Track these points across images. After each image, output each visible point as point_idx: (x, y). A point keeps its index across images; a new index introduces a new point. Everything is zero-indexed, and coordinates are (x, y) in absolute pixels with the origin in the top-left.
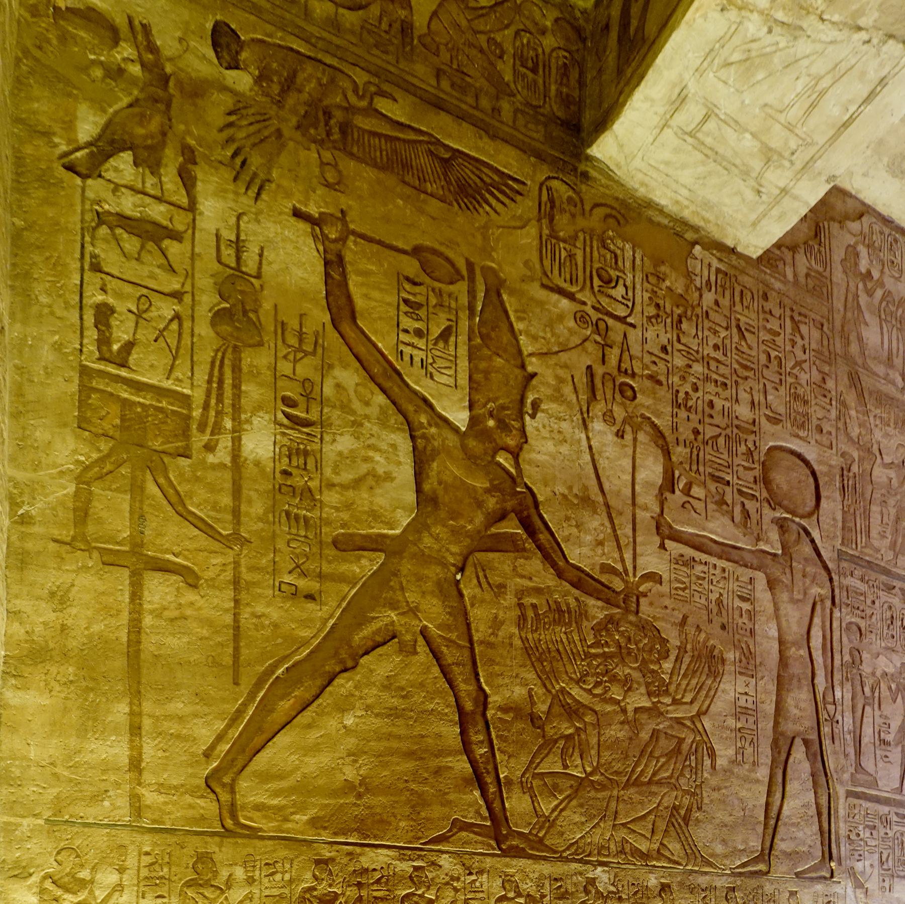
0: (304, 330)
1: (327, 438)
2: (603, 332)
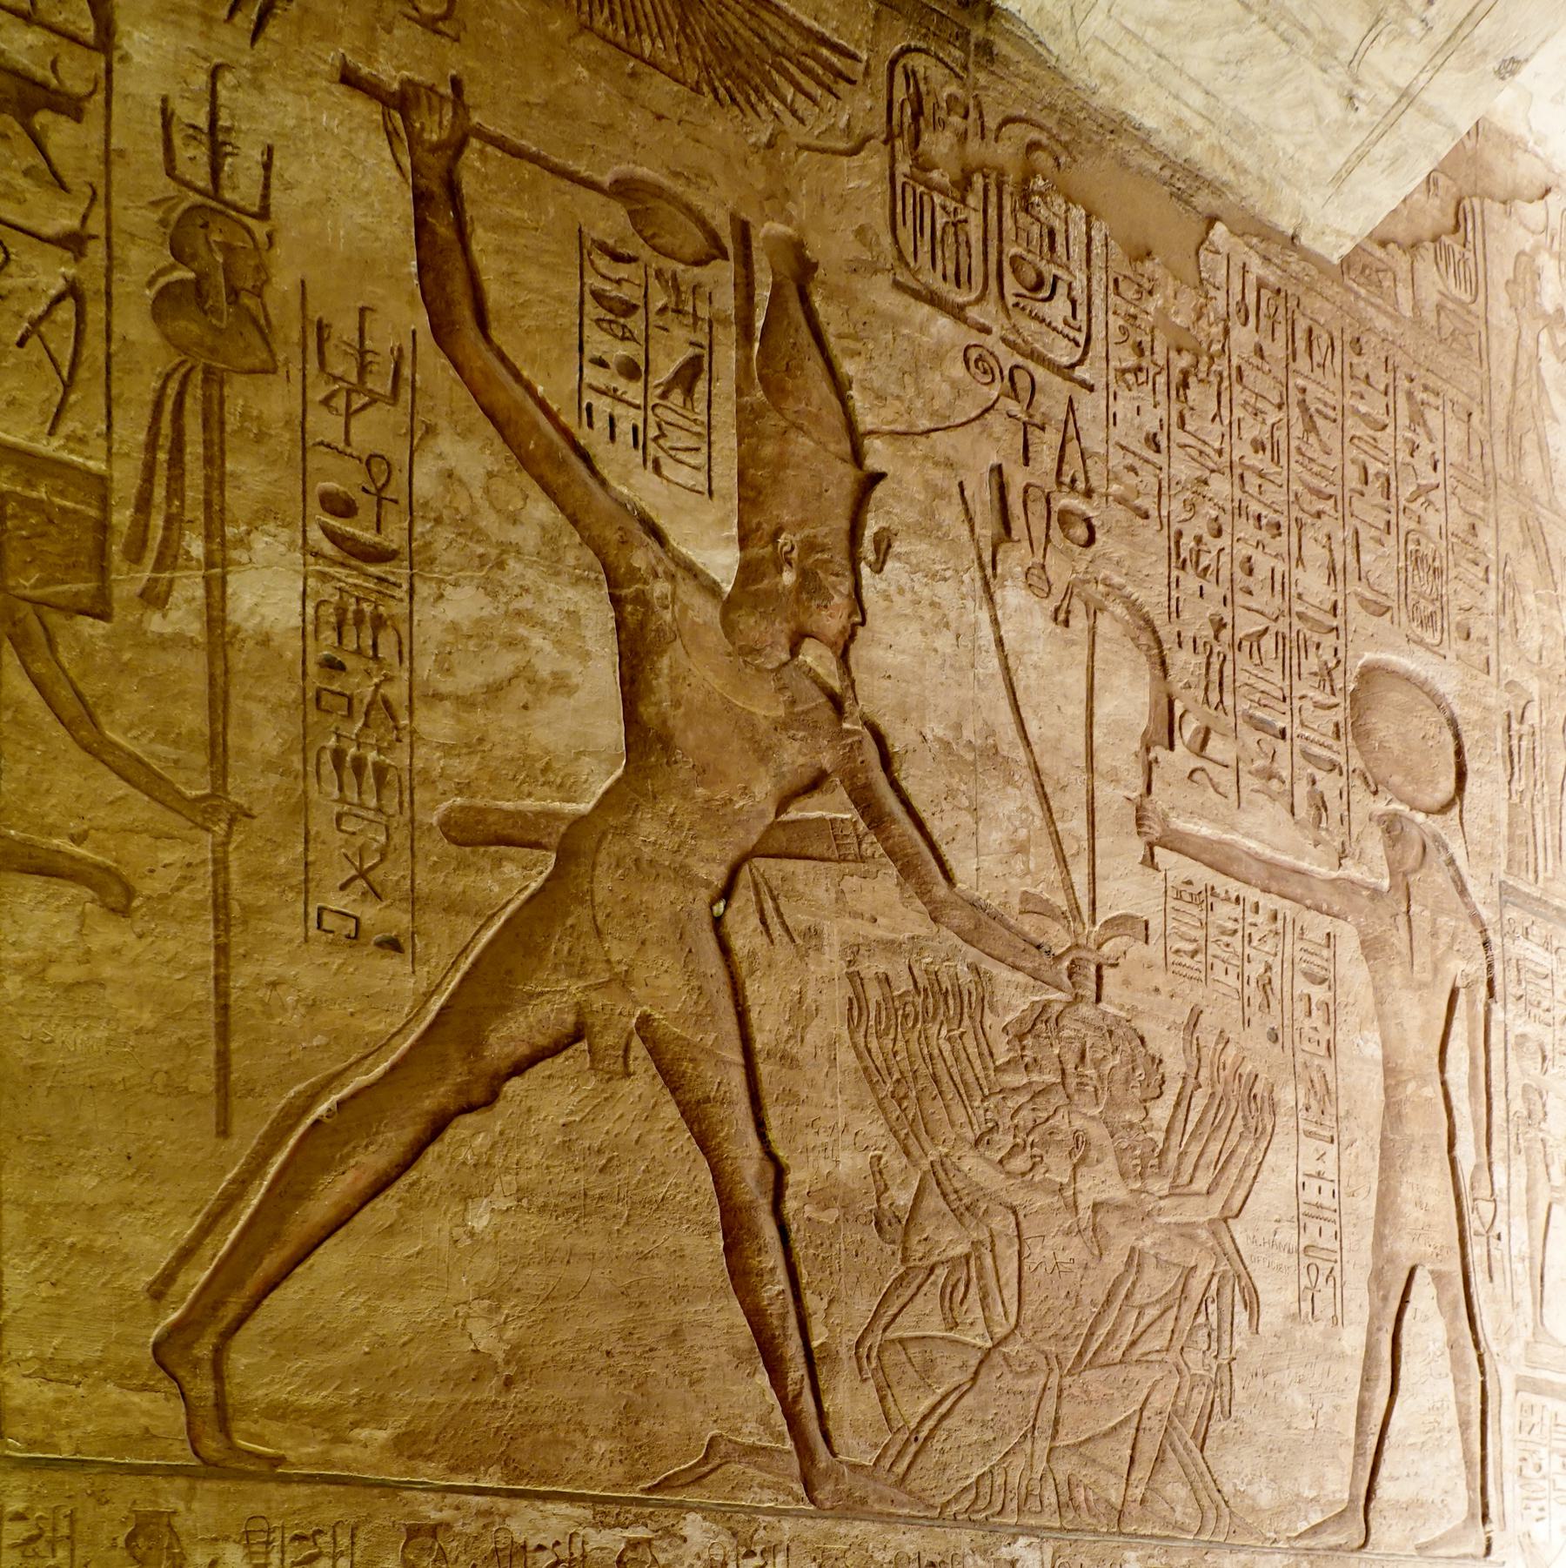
0: (368, 344)
1: (423, 590)
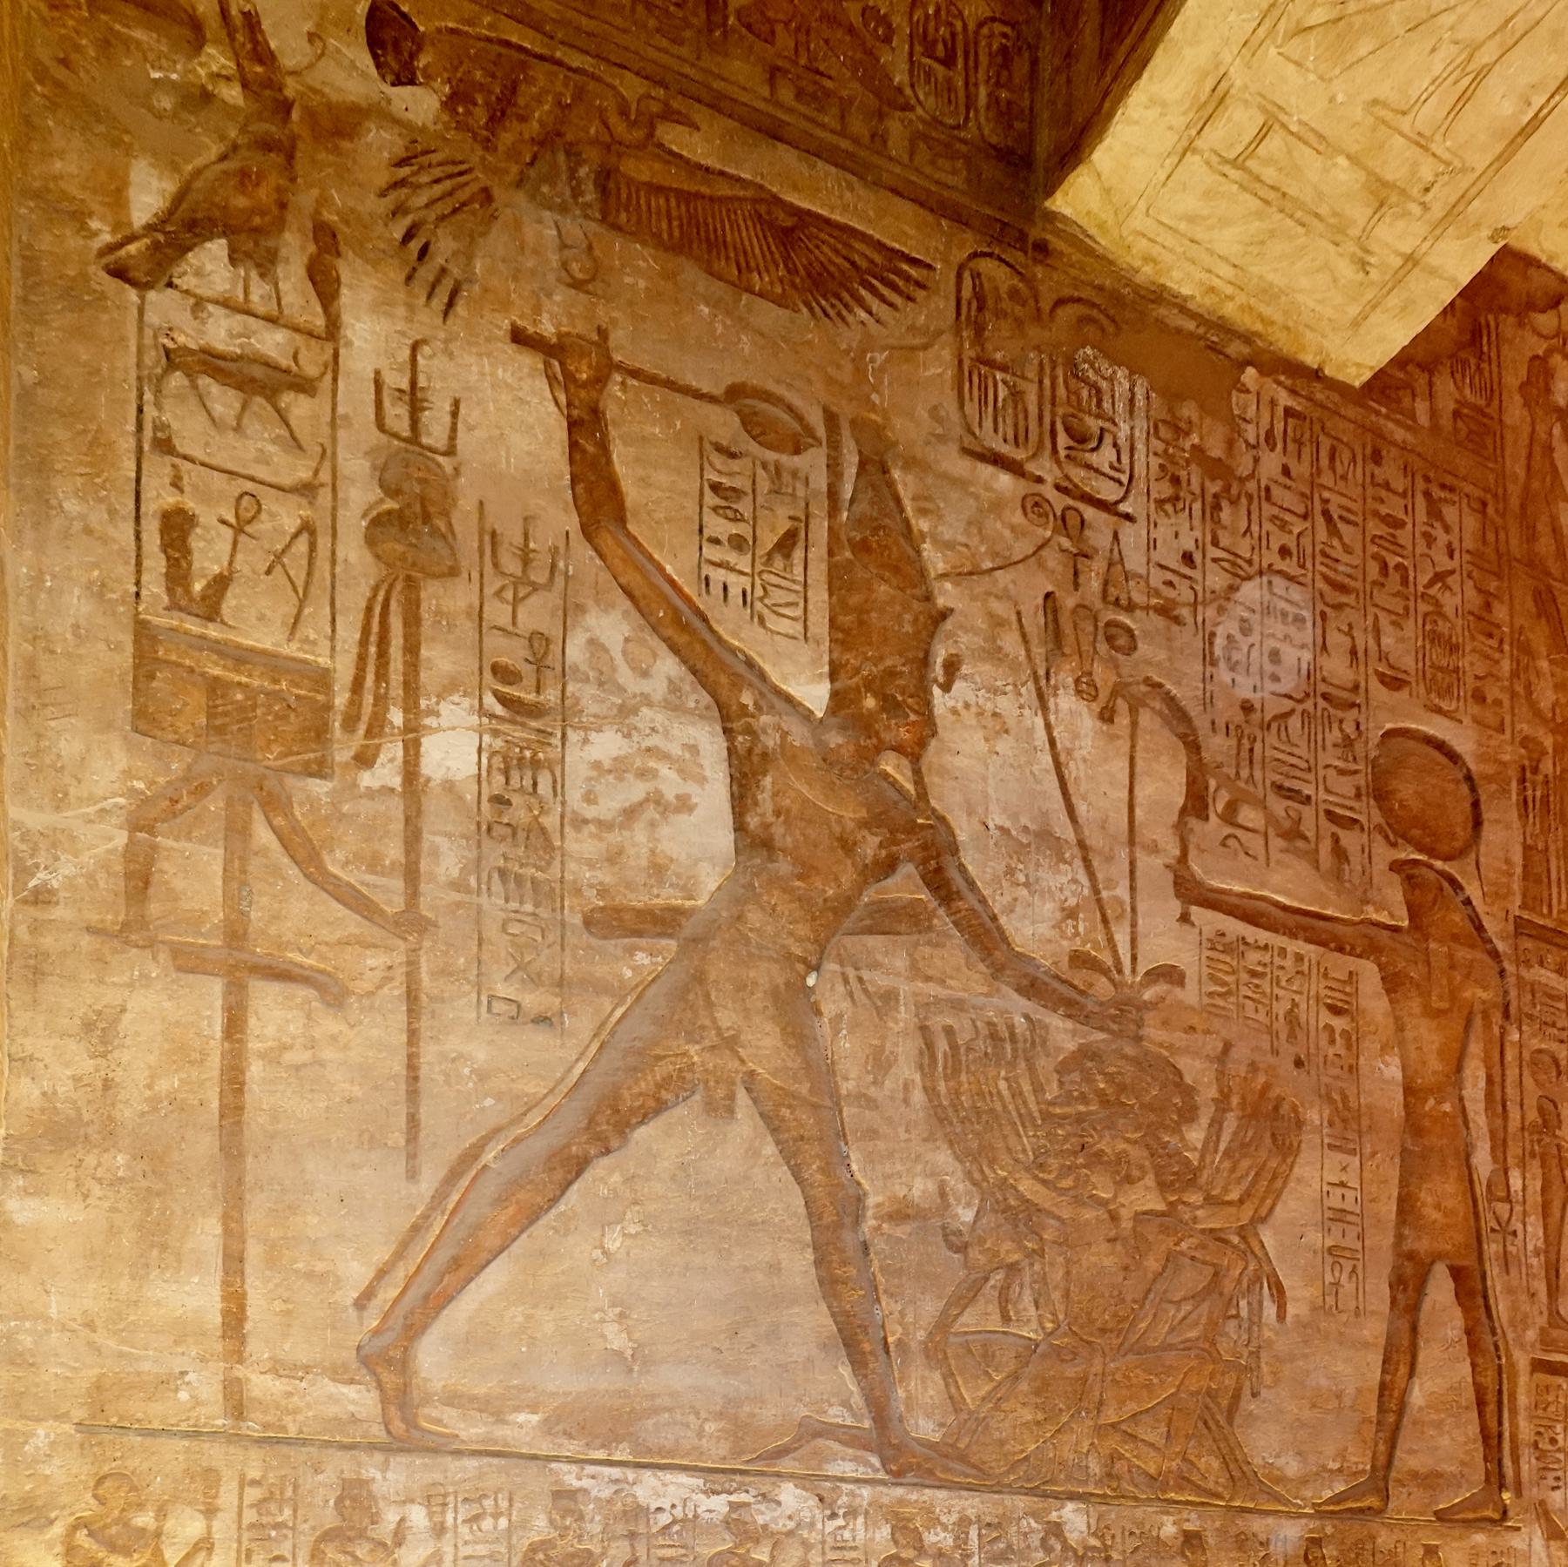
2: (1074, 532)
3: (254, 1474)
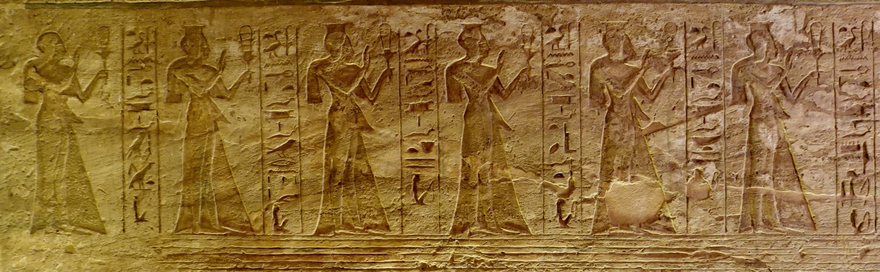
3: (130, 28)
